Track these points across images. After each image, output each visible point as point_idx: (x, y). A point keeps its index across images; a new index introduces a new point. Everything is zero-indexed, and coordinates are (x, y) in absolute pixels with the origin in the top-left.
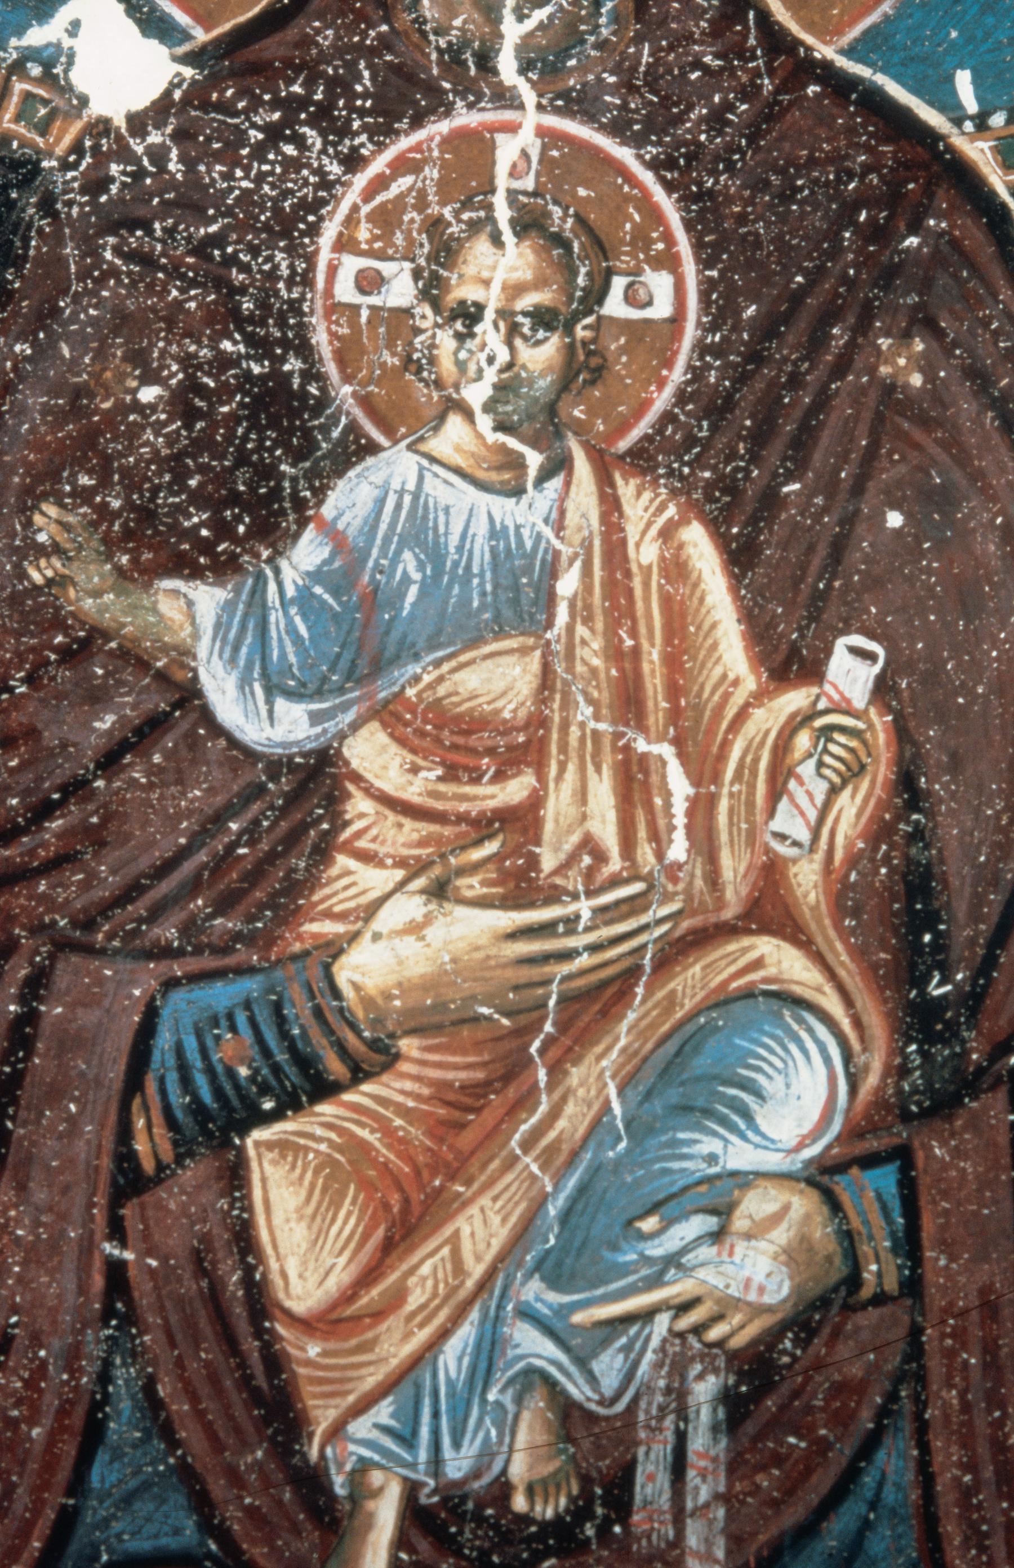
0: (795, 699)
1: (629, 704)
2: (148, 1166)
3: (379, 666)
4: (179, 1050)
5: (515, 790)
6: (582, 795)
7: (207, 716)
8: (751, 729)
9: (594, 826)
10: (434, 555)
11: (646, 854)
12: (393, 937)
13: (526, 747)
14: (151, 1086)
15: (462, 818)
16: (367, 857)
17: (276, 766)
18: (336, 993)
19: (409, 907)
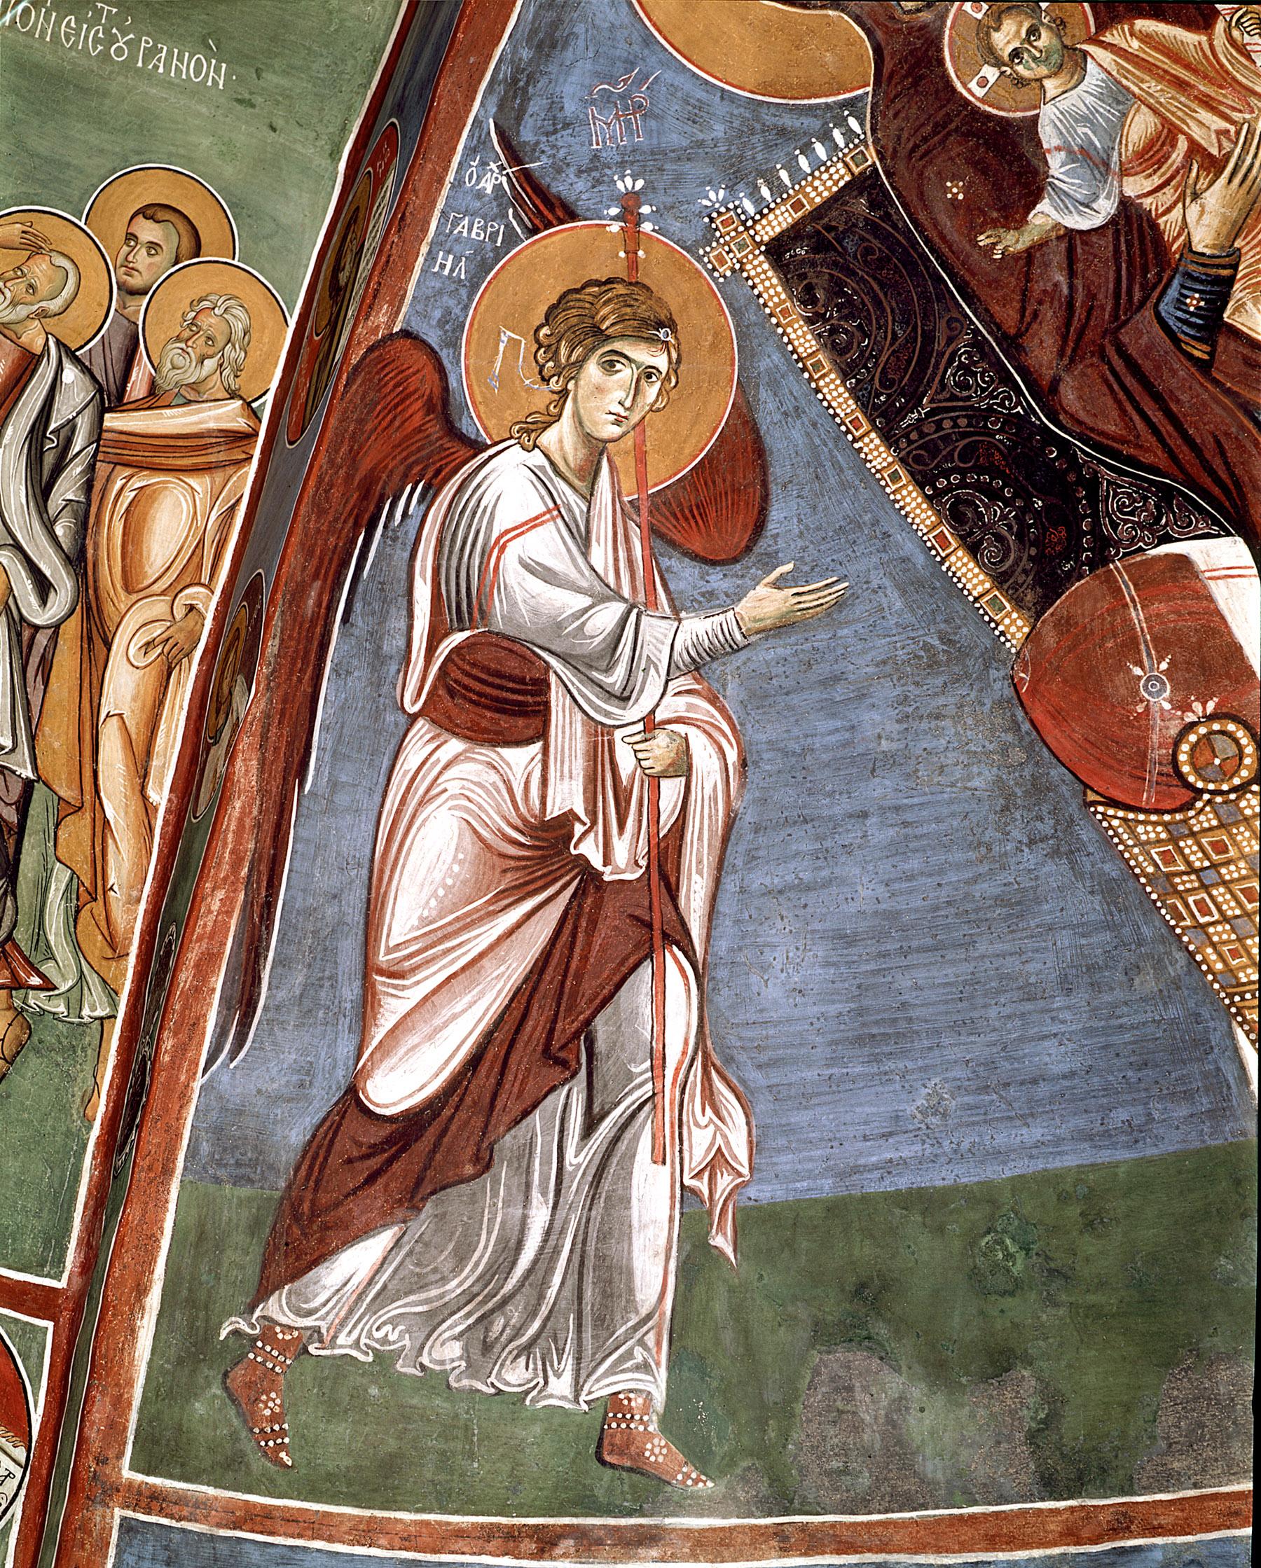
0: (1220, 26)
1: (1181, 85)
2: (1206, 357)
3: (1107, 165)
4: (1178, 318)
5: (1182, 144)
6: (1201, 123)
7: (1081, 232)
8: (1219, 50)
9: (1214, 127)
10: (1085, 120)
11: (1236, 116)
12: (1201, 223)
13: (1169, 133)
14: (1182, 336)
15: (1177, 171)
16: (1168, 210)
17: (1113, 221)
18: (1203, 254)
19: (1193, 210)
